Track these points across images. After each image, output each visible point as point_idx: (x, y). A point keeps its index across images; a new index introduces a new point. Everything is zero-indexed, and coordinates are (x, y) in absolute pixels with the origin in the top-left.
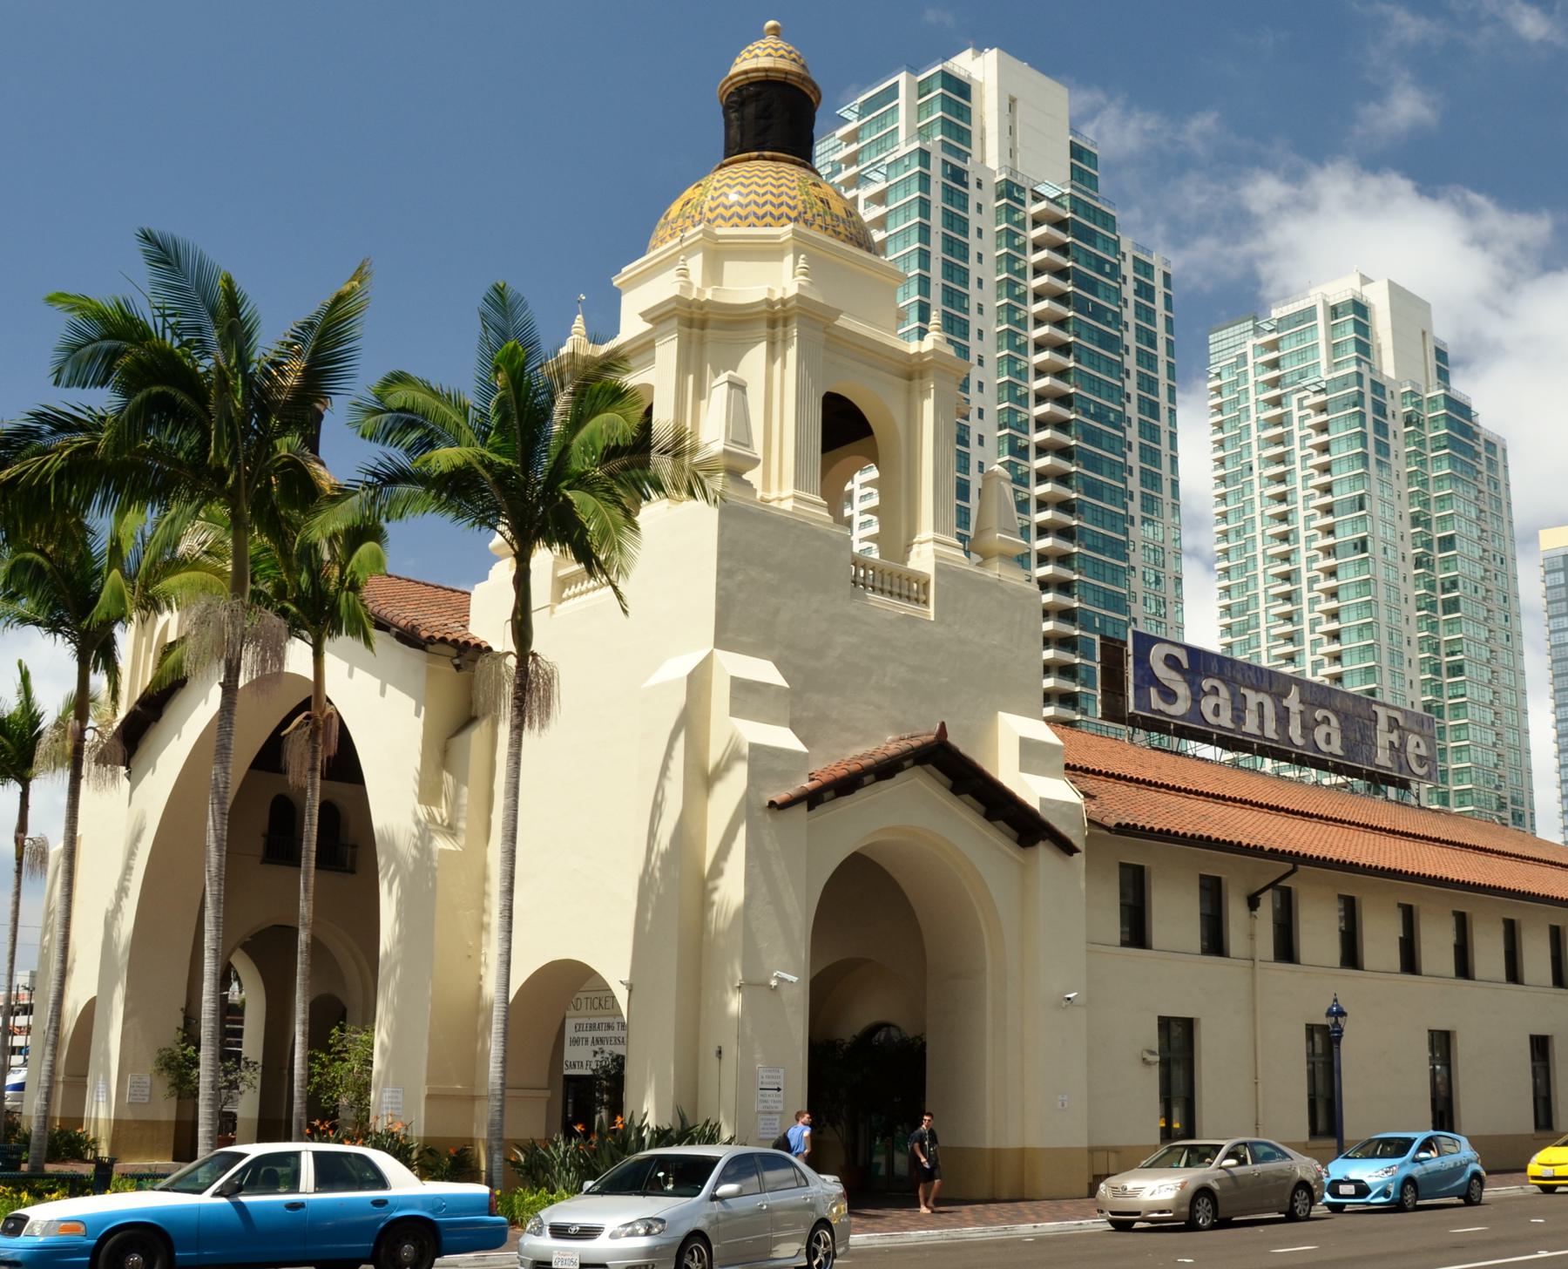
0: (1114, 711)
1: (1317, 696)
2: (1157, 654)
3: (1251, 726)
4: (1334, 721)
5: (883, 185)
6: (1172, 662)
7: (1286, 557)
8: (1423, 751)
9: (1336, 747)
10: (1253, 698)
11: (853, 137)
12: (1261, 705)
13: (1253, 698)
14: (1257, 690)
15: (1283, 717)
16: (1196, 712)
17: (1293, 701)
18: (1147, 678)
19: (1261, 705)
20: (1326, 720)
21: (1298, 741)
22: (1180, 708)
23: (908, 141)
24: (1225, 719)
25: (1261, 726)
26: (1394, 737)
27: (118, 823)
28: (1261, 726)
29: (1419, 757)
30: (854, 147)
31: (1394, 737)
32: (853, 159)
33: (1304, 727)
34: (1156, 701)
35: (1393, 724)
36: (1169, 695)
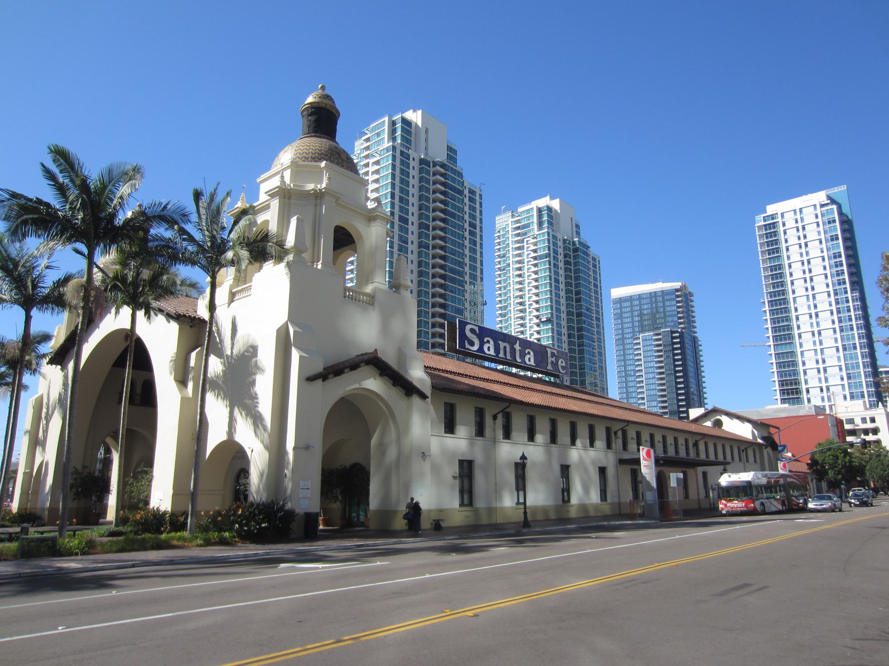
0: (452, 349)
1: (525, 344)
2: (468, 327)
3: (501, 355)
4: (532, 353)
5: (378, 158)
6: (472, 331)
7: (521, 297)
8: (564, 364)
9: (532, 363)
10: (502, 344)
11: (368, 140)
12: (505, 347)
13: (502, 344)
14: (504, 341)
15: (513, 351)
16: (481, 349)
17: (517, 347)
18: (463, 336)
19: (505, 347)
20: (529, 353)
21: (519, 360)
22: (476, 348)
23: (388, 142)
24: (492, 352)
25: (505, 354)
26: (553, 359)
27: (49, 382)
28: (505, 354)
29: (563, 368)
30: (368, 144)
31: (553, 359)
32: (367, 148)
33: (520, 356)
34: (467, 346)
35: (553, 355)
36: (472, 344)
